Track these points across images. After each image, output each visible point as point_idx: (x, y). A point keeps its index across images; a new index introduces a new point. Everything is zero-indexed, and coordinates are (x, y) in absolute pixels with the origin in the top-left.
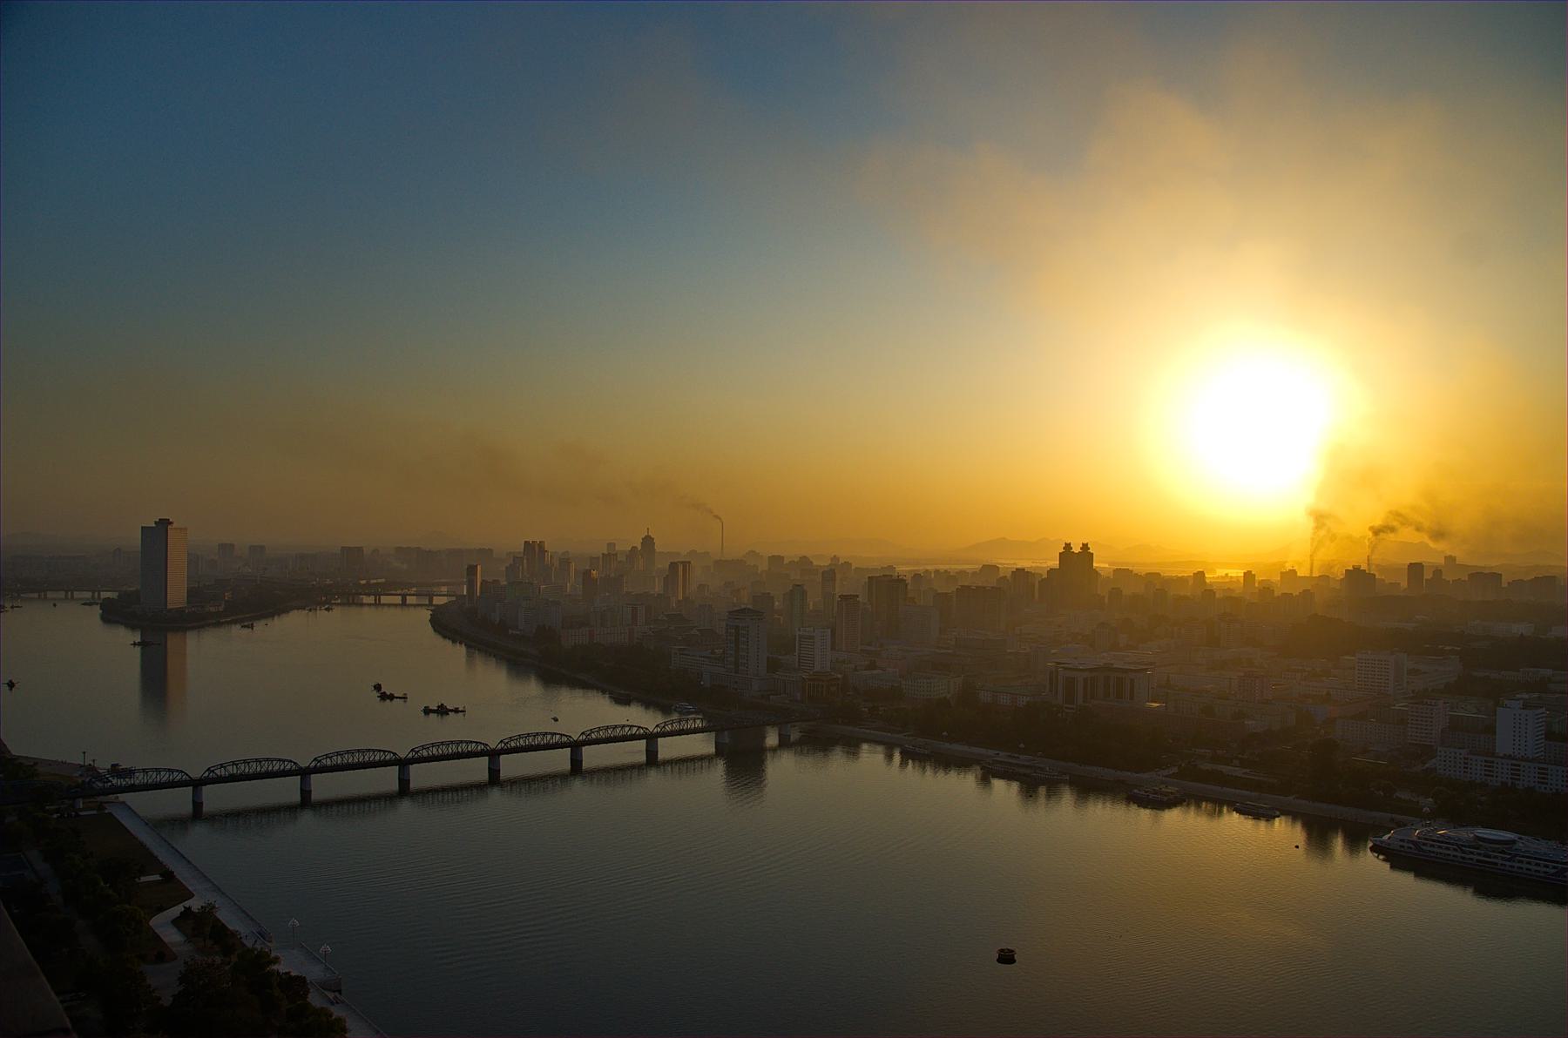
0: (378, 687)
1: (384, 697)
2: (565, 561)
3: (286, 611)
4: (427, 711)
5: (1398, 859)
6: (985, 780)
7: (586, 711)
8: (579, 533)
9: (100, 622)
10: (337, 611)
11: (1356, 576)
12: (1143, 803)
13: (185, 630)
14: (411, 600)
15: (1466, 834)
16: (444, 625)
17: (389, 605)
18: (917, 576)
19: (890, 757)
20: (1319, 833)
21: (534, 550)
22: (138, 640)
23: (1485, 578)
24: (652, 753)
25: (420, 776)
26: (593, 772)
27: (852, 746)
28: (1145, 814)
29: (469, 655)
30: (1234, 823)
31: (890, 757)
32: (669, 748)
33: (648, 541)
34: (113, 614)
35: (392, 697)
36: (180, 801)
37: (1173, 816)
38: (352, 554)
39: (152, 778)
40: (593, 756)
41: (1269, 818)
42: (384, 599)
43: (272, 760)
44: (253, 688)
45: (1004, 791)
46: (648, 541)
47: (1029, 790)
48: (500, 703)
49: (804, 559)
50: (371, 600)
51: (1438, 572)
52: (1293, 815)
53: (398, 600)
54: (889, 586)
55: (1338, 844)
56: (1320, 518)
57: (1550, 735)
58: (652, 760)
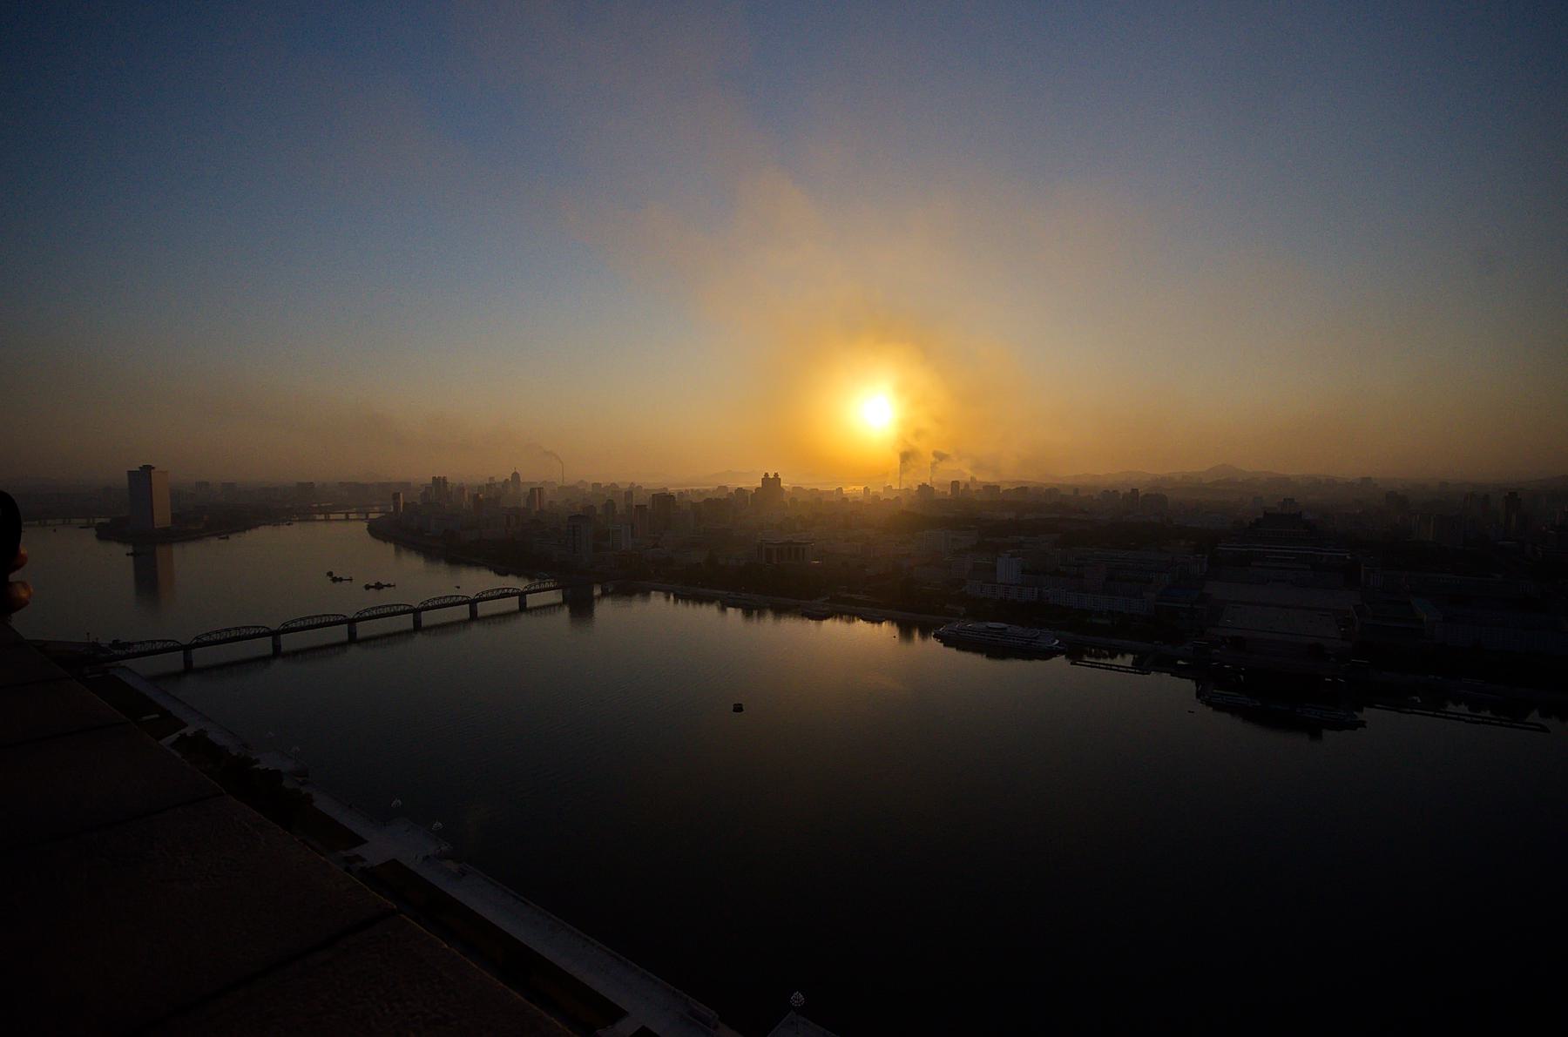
0: (330, 574)
1: (335, 580)
2: (461, 489)
3: (256, 526)
4: (368, 587)
5: (947, 641)
6: (723, 609)
7: (478, 580)
8: (469, 468)
10: (296, 525)
11: (923, 487)
12: (812, 618)
15: (982, 626)
16: (376, 531)
18: (681, 493)
19: (668, 598)
20: (906, 631)
21: (439, 482)
23: (991, 489)
24: (523, 604)
26: (485, 618)
27: (646, 593)
28: (812, 623)
29: (397, 550)
30: (861, 626)
31: (668, 598)
32: (533, 600)
33: (516, 475)
36: (175, 661)
37: (828, 624)
38: (306, 488)
40: (484, 609)
41: (880, 622)
42: (332, 516)
45: (734, 614)
46: (516, 475)
47: (748, 613)
48: (418, 579)
49: (613, 485)
51: (967, 485)
52: (891, 619)
54: (664, 500)
55: (916, 634)
56: (906, 457)
57: (1023, 571)
58: (523, 608)
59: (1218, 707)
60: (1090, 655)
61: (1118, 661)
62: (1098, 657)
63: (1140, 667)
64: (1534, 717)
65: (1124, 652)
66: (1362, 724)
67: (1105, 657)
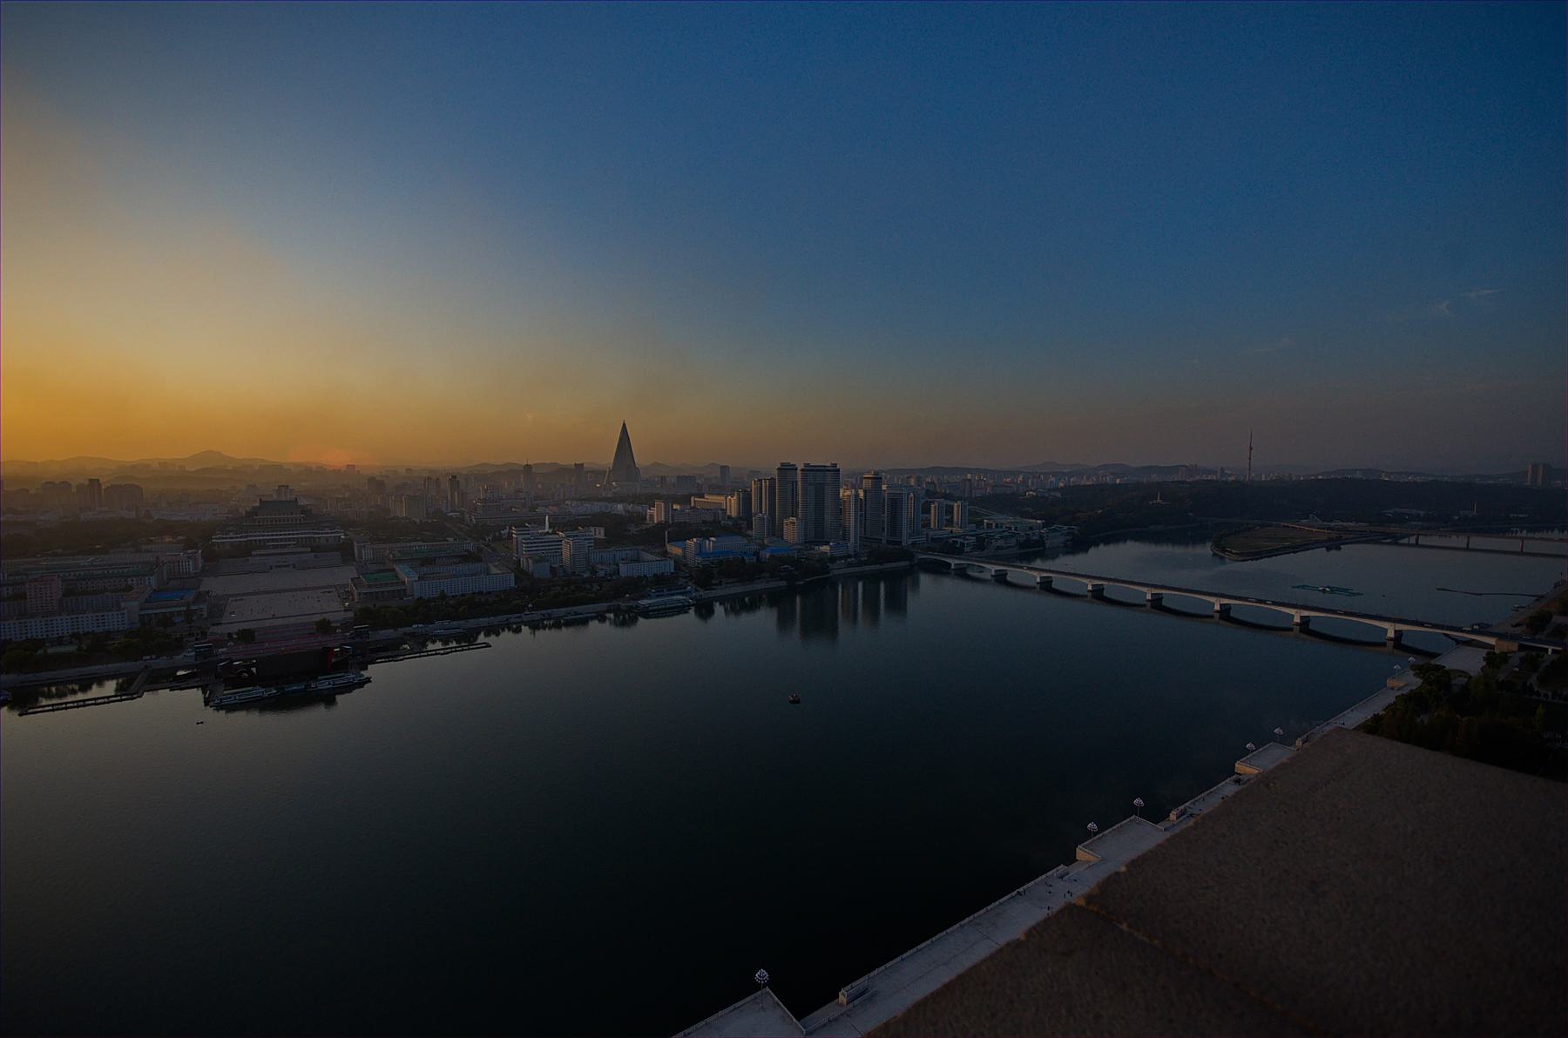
59: (231, 708)
60: (49, 696)
61: (95, 692)
62: (61, 695)
63: (127, 691)
64: (481, 638)
65: (100, 681)
66: (368, 680)
67: (74, 692)
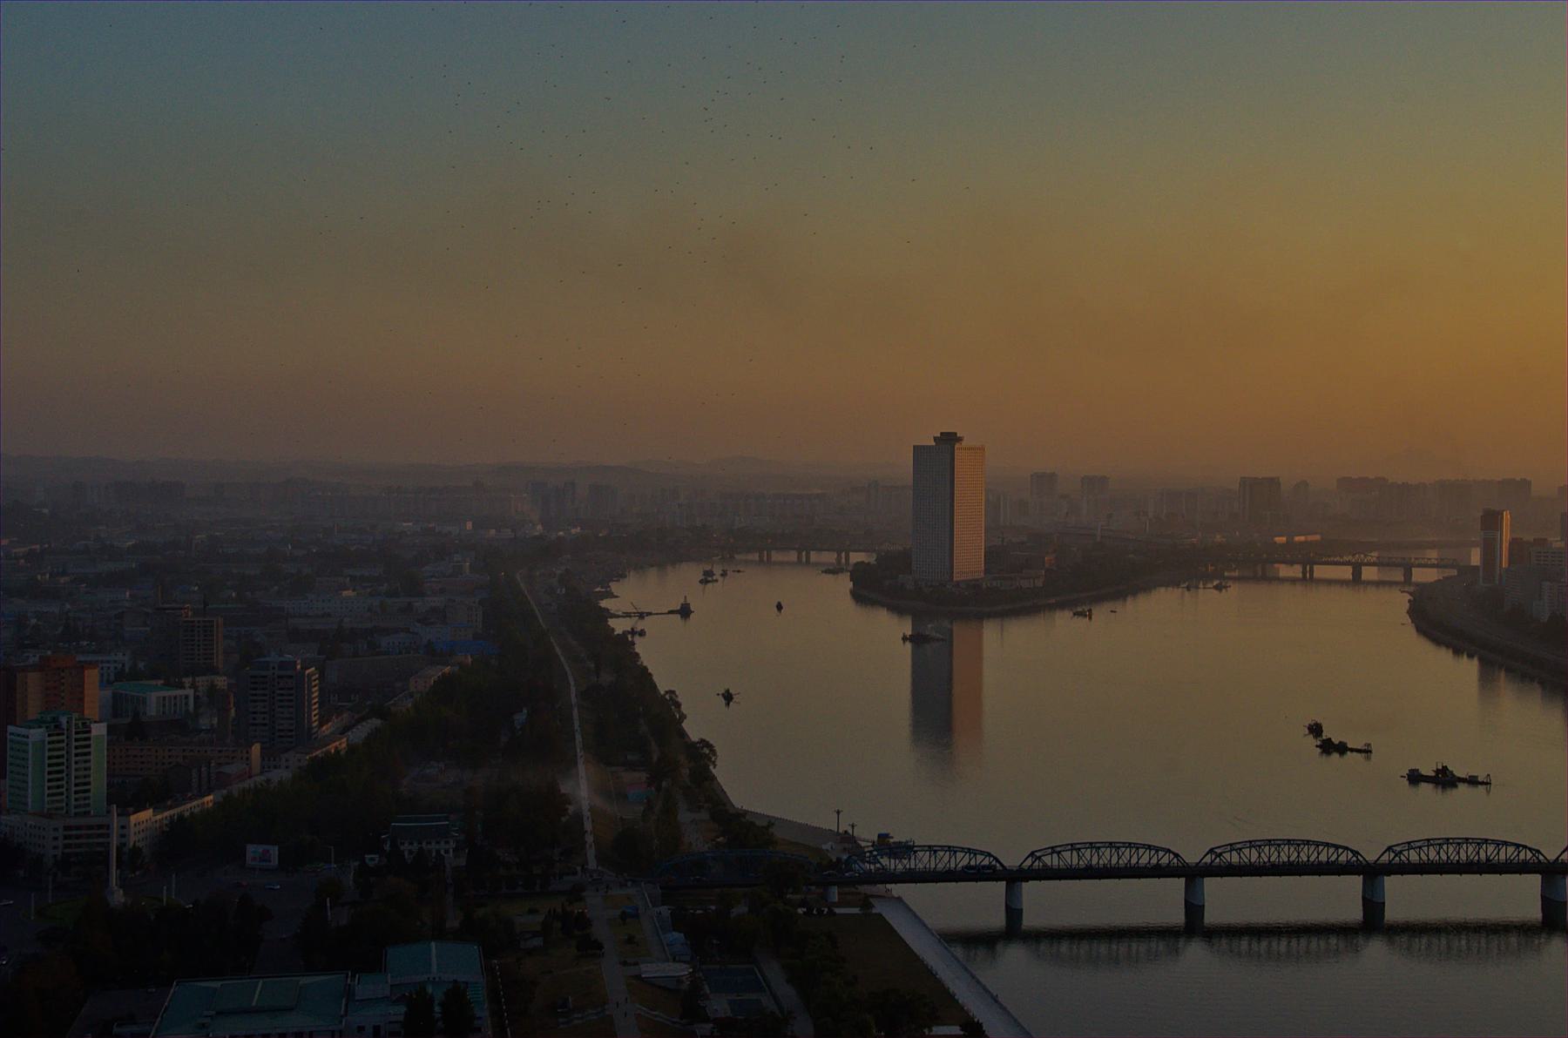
0: (1316, 730)
1: (1328, 747)
4: (1415, 778)
9: (848, 602)
10: (1234, 590)
13: (980, 617)
14: (1369, 573)
17: (1329, 582)
22: (909, 633)
25: (1406, 898)
34: (872, 588)
35: (1342, 749)
38: (1260, 490)
39: (944, 861)
42: (1320, 571)
43: (1137, 846)
44: (1105, 723)
50: (1296, 571)
53: (1346, 573)
